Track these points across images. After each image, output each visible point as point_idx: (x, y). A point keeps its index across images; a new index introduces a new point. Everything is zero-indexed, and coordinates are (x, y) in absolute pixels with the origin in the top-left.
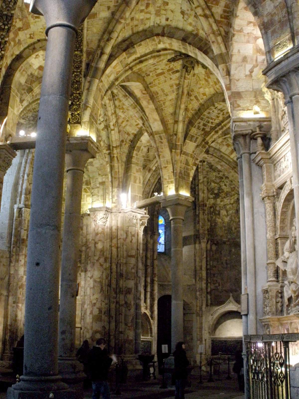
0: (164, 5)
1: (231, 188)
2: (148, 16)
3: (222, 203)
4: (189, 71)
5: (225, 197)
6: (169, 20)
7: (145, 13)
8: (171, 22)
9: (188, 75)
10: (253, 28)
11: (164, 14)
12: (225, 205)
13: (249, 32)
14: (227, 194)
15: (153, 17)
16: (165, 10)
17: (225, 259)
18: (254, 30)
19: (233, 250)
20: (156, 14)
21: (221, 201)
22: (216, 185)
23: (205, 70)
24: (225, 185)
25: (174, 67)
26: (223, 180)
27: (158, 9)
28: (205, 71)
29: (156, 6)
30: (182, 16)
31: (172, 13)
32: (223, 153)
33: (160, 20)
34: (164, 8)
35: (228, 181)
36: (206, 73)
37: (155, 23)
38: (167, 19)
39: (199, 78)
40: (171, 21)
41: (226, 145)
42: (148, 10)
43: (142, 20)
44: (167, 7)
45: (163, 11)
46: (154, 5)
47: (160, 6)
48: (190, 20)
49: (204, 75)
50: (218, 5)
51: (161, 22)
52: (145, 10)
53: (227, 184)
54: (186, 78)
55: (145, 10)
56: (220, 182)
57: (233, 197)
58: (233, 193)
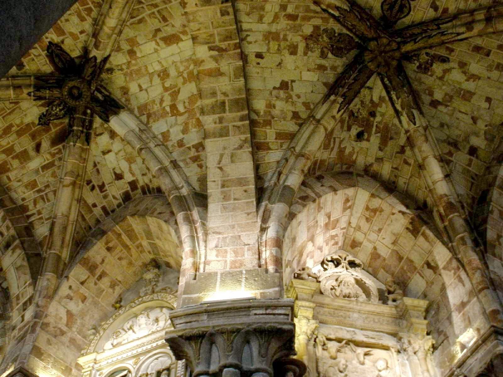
0: (289, 46)
2: (268, 18)
4: (38, 94)
6: (259, 60)
7: (276, 13)
8: (255, 64)
9: (29, 94)
10: (322, 225)
11: (268, 50)
13: (319, 223)
15: (264, 27)
16: (278, 50)
18: (321, 227)
20: (270, 33)
23: (37, 122)
25: (32, 56)
27: (282, 36)
28: (33, 123)
29: (288, 33)
30: (278, 85)
31: (277, 63)
33: (255, 42)
34: (282, 47)
36: (28, 125)
37: (248, 33)
38: (259, 56)
39: (10, 114)
40: (258, 64)
42: (282, 19)
43: (263, 8)
44: (286, 53)
45: (276, 47)
46: (291, 28)
47: (287, 40)
48: (280, 105)
49: (22, 123)
50: (324, 149)
51: (250, 43)
52: (284, 13)
54: (18, 91)
55: (284, 13)
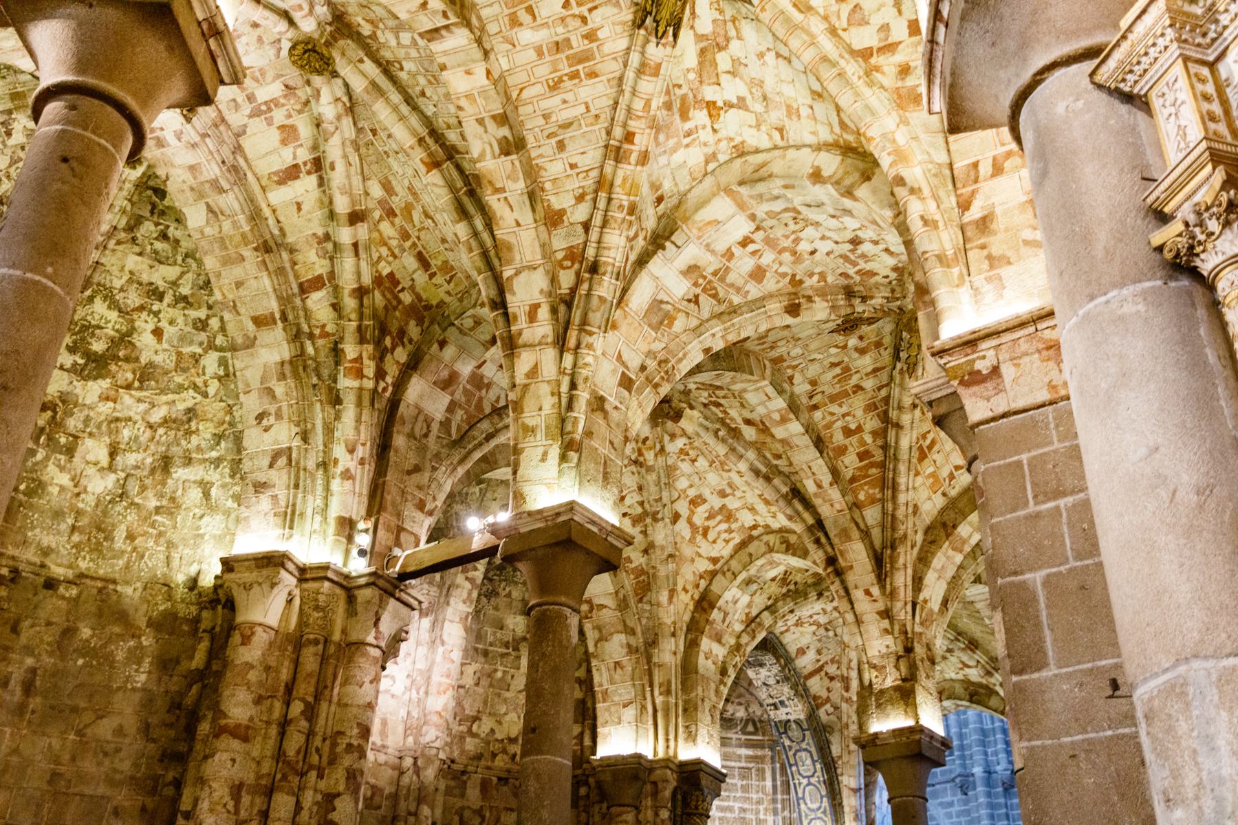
1: (179, 354)
3: (105, 408)
5: (128, 387)
12: (117, 420)
14: (146, 375)
17: (30, 661)
19: (86, 632)
21: (105, 398)
22: (113, 315)
24: (158, 333)
26: (155, 308)
32: (246, 160)
35: (180, 320)
41: (282, 128)
53: (169, 331)
56: (141, 308)
57: (171, 397)
58: (179, 379)
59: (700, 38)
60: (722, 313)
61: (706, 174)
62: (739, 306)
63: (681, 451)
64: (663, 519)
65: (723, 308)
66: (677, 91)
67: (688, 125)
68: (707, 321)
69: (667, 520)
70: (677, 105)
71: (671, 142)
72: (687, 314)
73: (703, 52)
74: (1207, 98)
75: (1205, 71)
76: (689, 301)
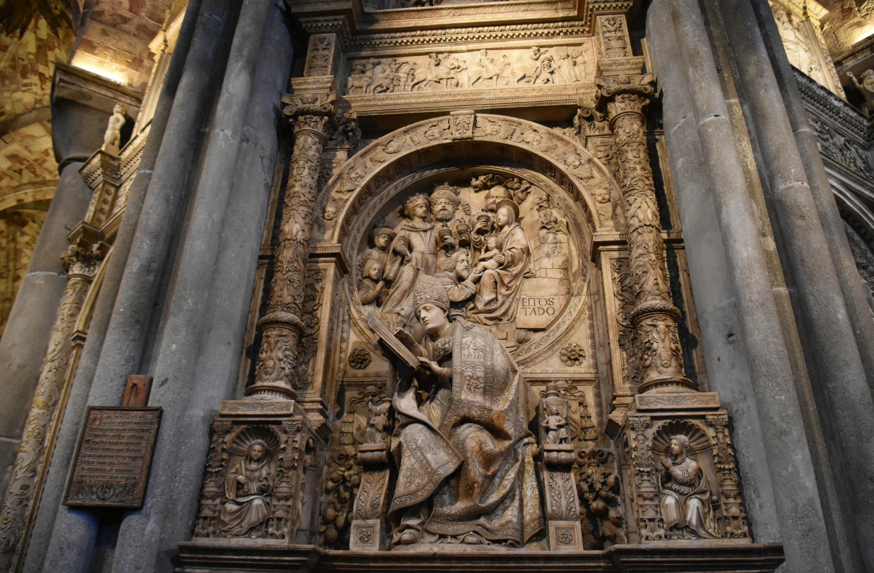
59: (38, 39)
60: (36, 183)
61: (34, 109)
62: (49, 181)
63: (27, 243)
64: (6, 278)
65: (38, 180)
66: (21, 62)
67: (26, 81)
68: (25, 184)
69: (10, 279)
70: (19, 68)
71: (13, 87)
72: (12, 178)
73: (39, 48)
74: (105, 202)
75: (113, 190)
76: (15, 171)
